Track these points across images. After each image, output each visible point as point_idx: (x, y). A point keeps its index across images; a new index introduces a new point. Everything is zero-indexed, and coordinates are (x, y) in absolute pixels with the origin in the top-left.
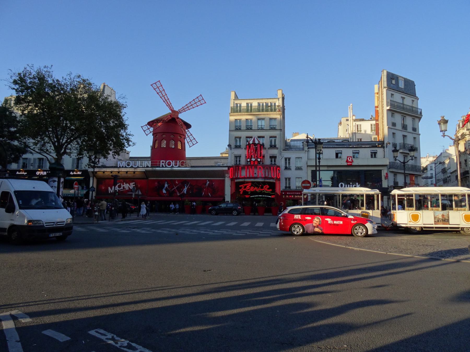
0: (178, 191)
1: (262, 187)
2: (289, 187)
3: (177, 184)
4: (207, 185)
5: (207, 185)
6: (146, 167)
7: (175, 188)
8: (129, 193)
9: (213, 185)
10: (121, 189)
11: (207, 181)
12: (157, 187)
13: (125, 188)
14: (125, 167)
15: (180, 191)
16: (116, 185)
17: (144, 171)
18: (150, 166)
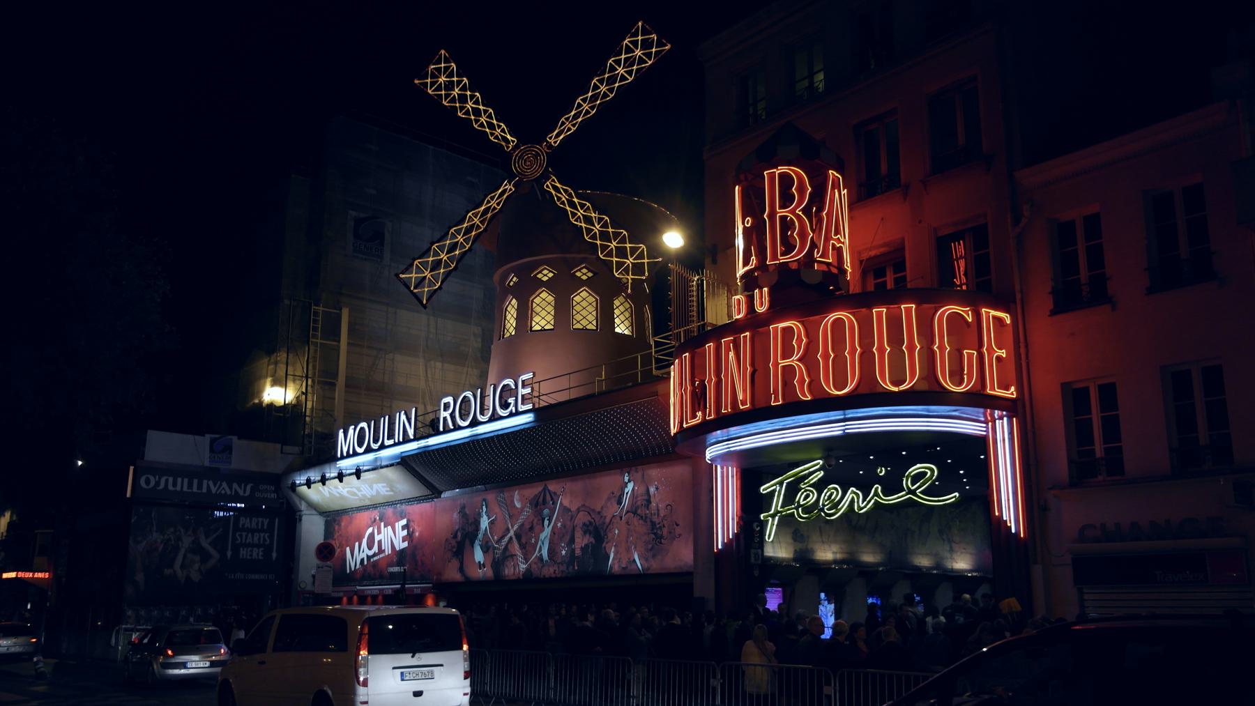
0: (523, 547)
1: (892, 486)
2: (1114, 462)
3: (522, 509)
4: (626, 501)
5: (626, 501)
6: (401, 440)
7: (512, 533)
8: (392, 570)
9: (649, 501)
10: (375, 555)
11: (626, 479)
12: (459, 534)
13: (383, 548)
14: (355, 454)
15: (527, 548)
16: (364, 537)
17: (398, 463)
18: (411, 432)
